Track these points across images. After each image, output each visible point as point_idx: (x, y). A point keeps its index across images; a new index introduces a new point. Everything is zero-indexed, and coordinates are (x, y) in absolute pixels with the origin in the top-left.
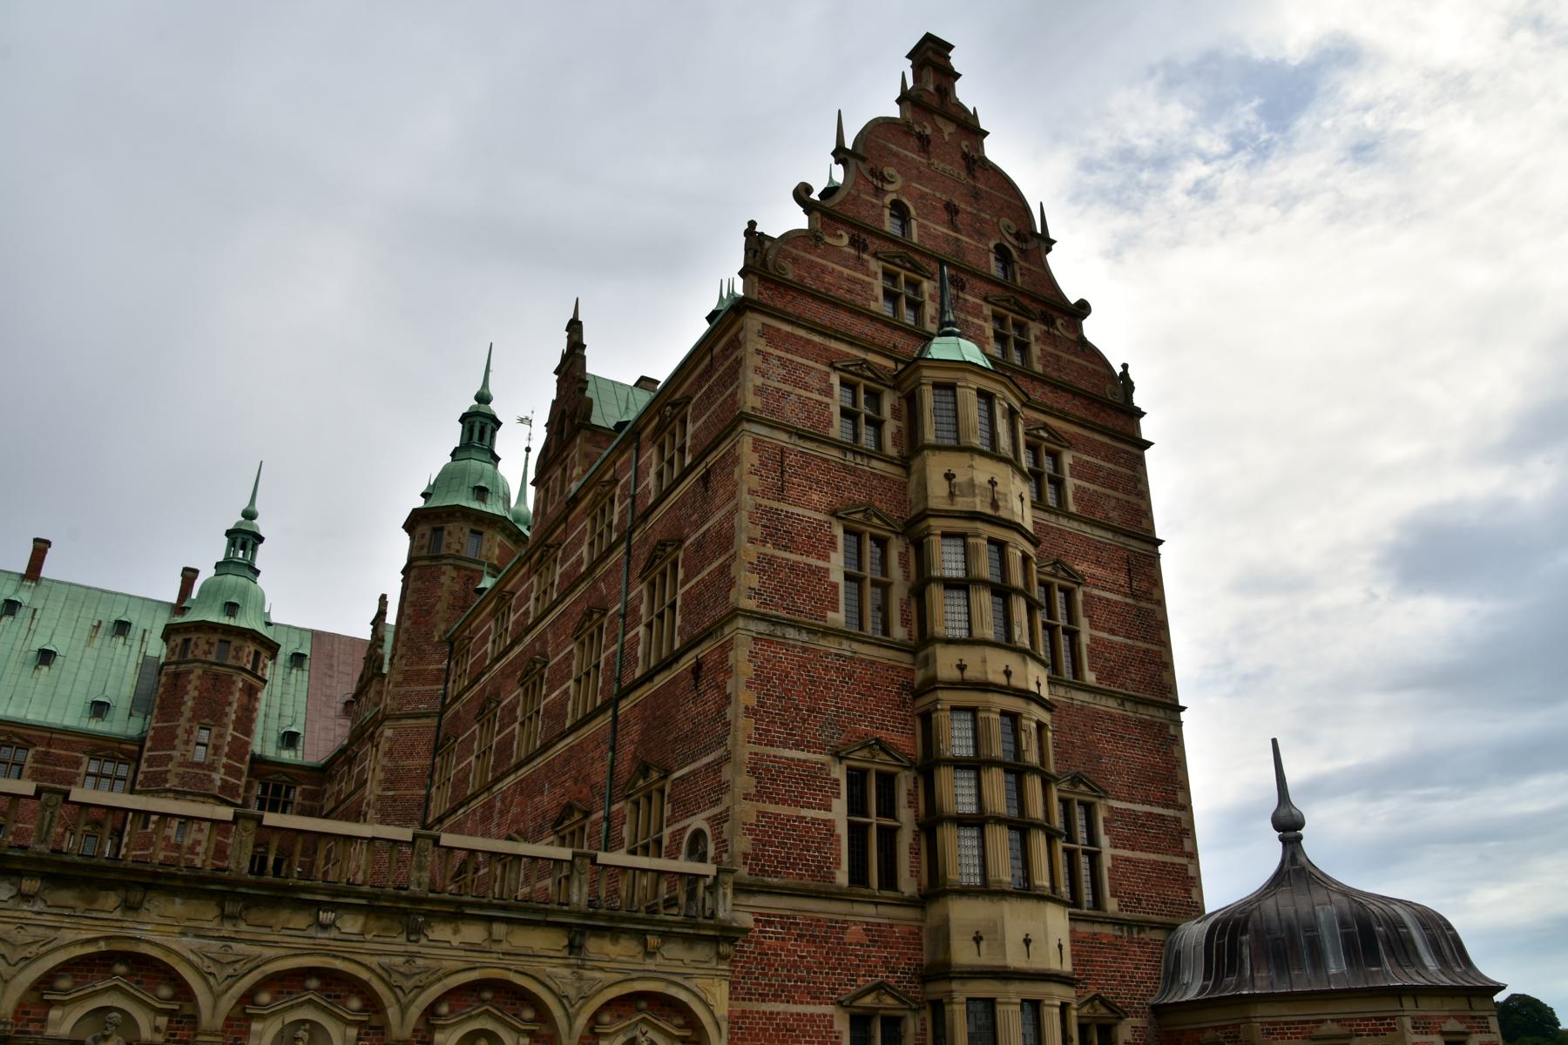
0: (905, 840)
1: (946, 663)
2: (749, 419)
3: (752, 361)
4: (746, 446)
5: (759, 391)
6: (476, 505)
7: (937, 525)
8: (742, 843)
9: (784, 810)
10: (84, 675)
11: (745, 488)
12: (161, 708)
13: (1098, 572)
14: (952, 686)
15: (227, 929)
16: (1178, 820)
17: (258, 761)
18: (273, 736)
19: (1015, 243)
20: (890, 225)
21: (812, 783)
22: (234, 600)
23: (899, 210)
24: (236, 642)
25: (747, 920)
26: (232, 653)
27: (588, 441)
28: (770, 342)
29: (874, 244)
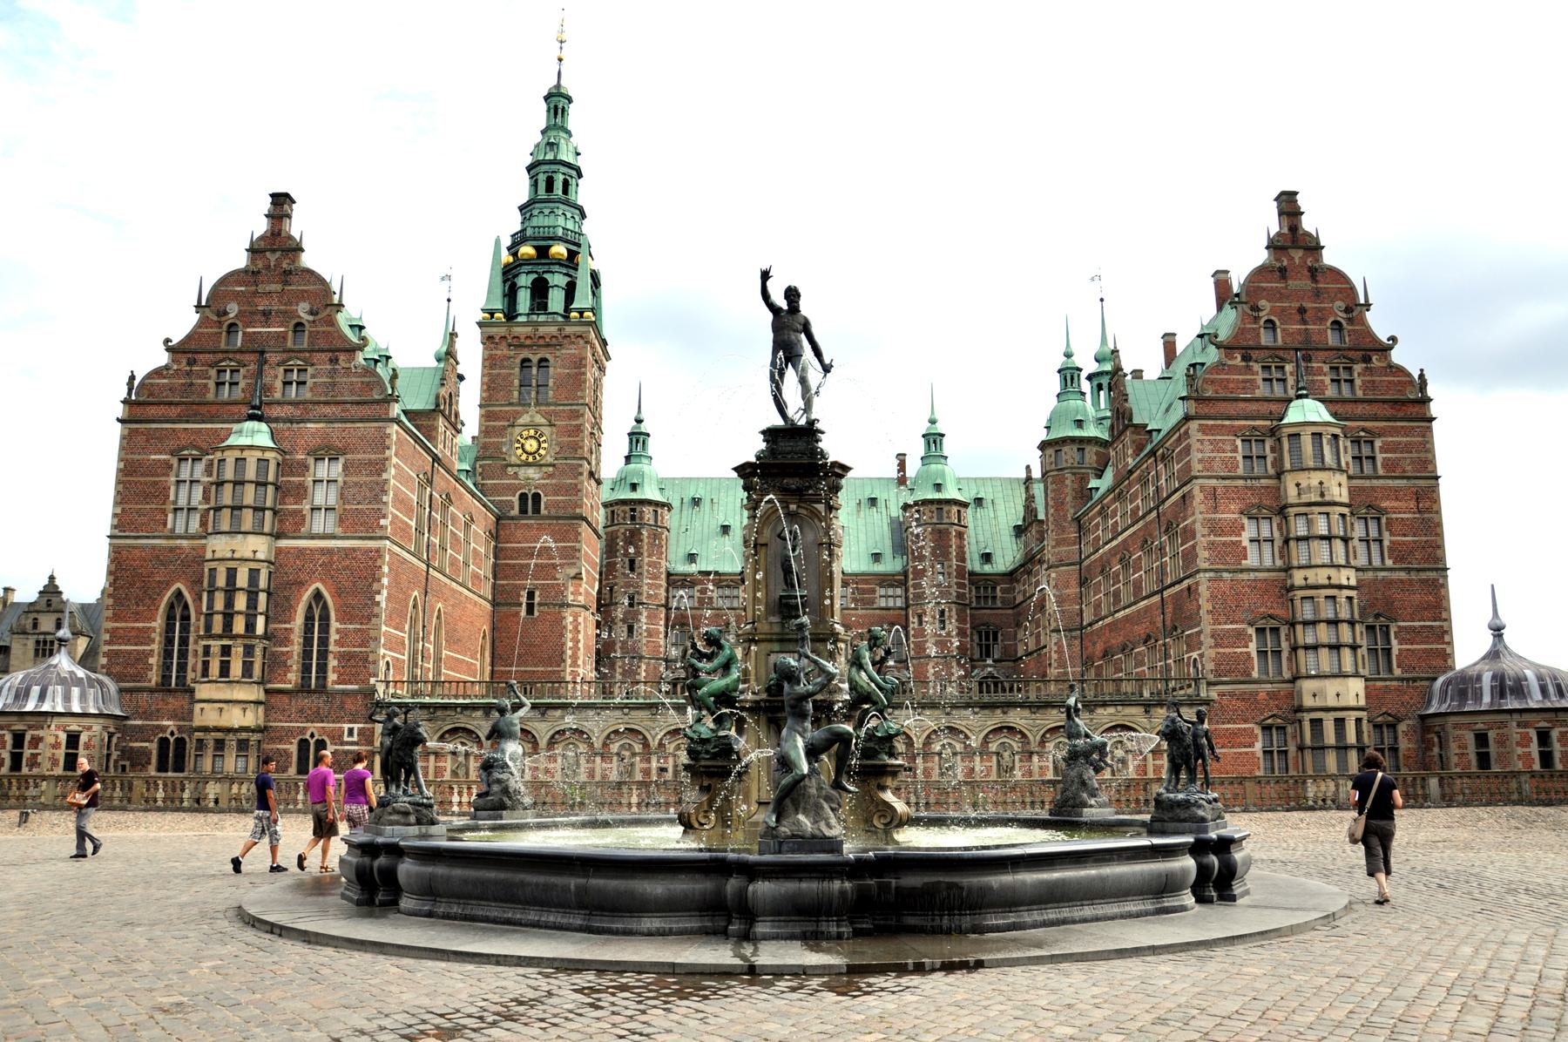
0: (1285, 655)
1: (1298, 578)
2: (1196, 478)
3: (1196, 446)
4: (1196, 491)
5: (1200, 461)
6: (1078, 433)
7: (1292, 511)
8: (1210, 666)
9: (1227, 650)
10: (862, 537)
11: (1197, 512)
13: (1396, 504)
14: (1301, 588)
15: (1033, 716)
16: (1442, 627)
17: (972, 574)
18: (976, 557)
19: (1344, 315)
20: (1265, 339)
21: (1241, 637)
22: (939, 481)
23: (1270, 325)
24: (946, 508)
25: (1214, 695)
26: (945, 515)
27: (1133, 433)
28: (1204, 433)
29: (1255, 354)
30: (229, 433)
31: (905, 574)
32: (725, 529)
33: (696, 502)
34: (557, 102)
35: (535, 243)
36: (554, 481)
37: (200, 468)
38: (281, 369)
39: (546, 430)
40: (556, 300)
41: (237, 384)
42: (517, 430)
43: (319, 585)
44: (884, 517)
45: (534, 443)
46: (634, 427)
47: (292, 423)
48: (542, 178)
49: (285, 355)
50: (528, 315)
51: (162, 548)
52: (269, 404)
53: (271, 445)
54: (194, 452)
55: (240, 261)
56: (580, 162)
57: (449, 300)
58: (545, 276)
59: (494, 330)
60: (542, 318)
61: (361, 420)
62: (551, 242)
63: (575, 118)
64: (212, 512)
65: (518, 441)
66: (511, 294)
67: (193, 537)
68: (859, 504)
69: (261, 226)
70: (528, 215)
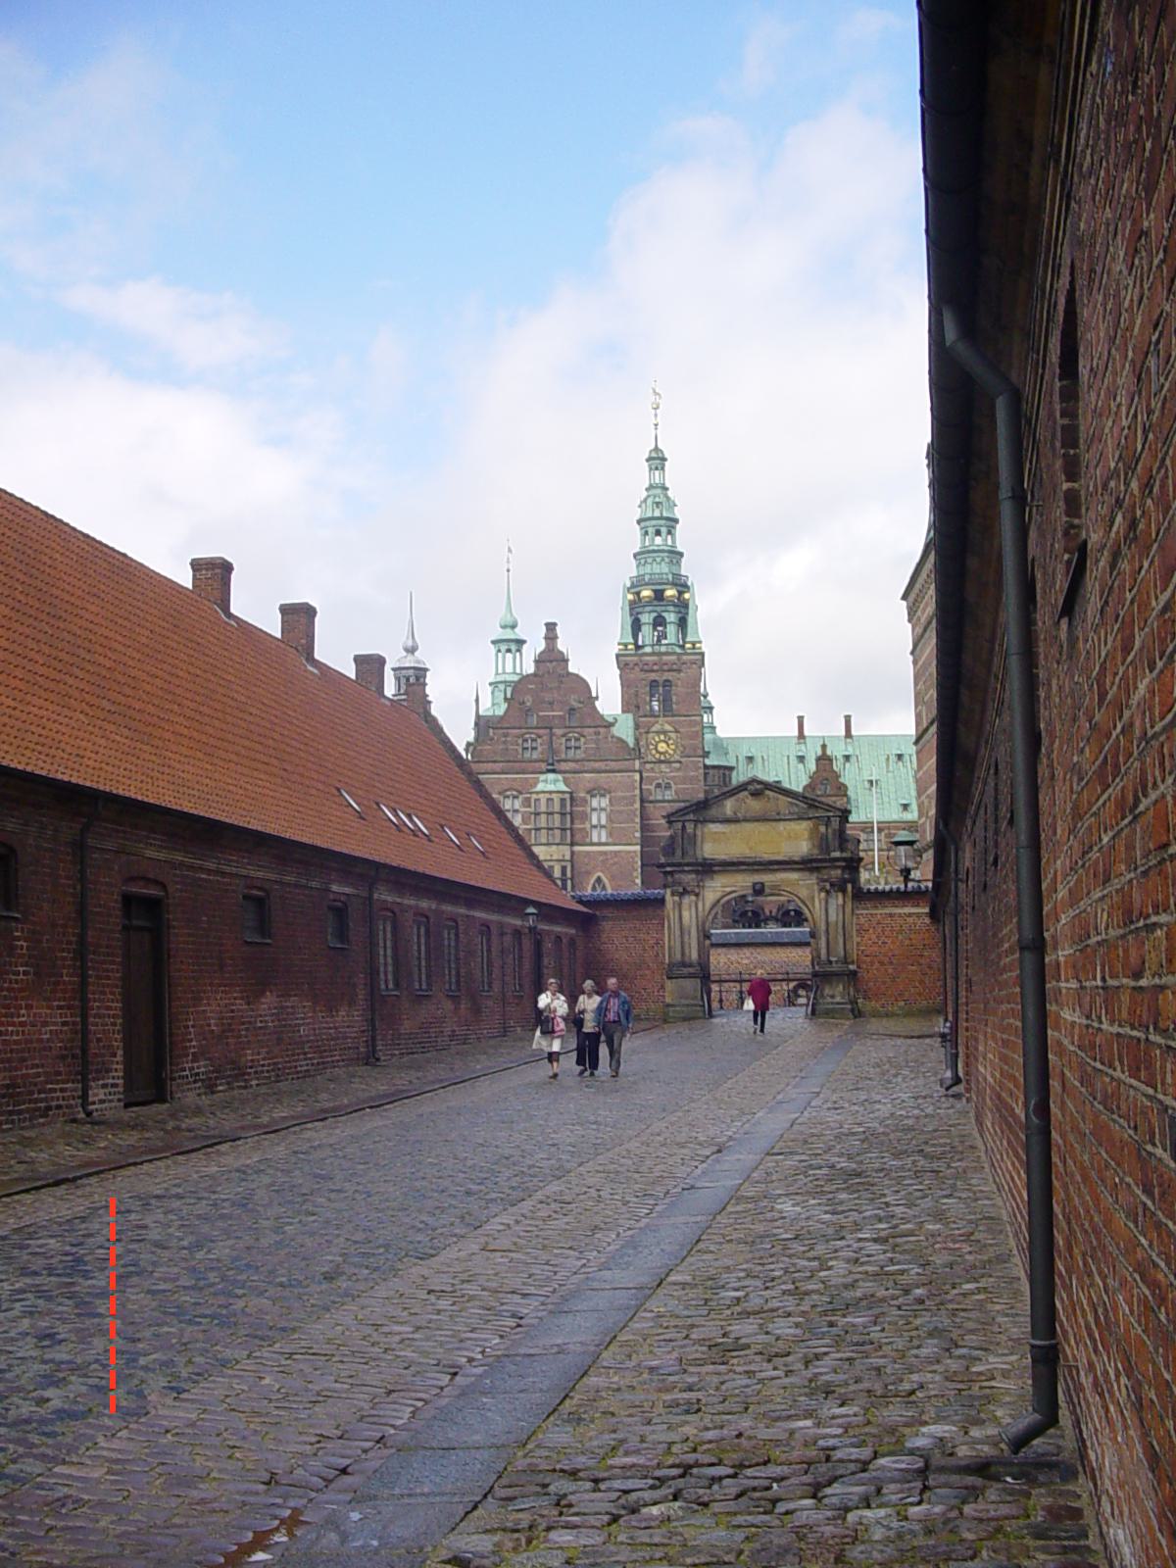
34: (657, 460)
35: (654, 587)
37: (517, 804)
38: (564, 740)
39: (673, 735)
40: (671, 630)
42: (651, 735)
43: (600, 874)
45: (664, 745)
48: (651, 530)
50: (653, 645)
52: (559, 761)
53: (565, 789)
56: (677, 514)
57: (508, 571)
58: (664, 614)
61: (618, 771)
63: (671, 476)
68: (888, 759)
70: (643, 561)
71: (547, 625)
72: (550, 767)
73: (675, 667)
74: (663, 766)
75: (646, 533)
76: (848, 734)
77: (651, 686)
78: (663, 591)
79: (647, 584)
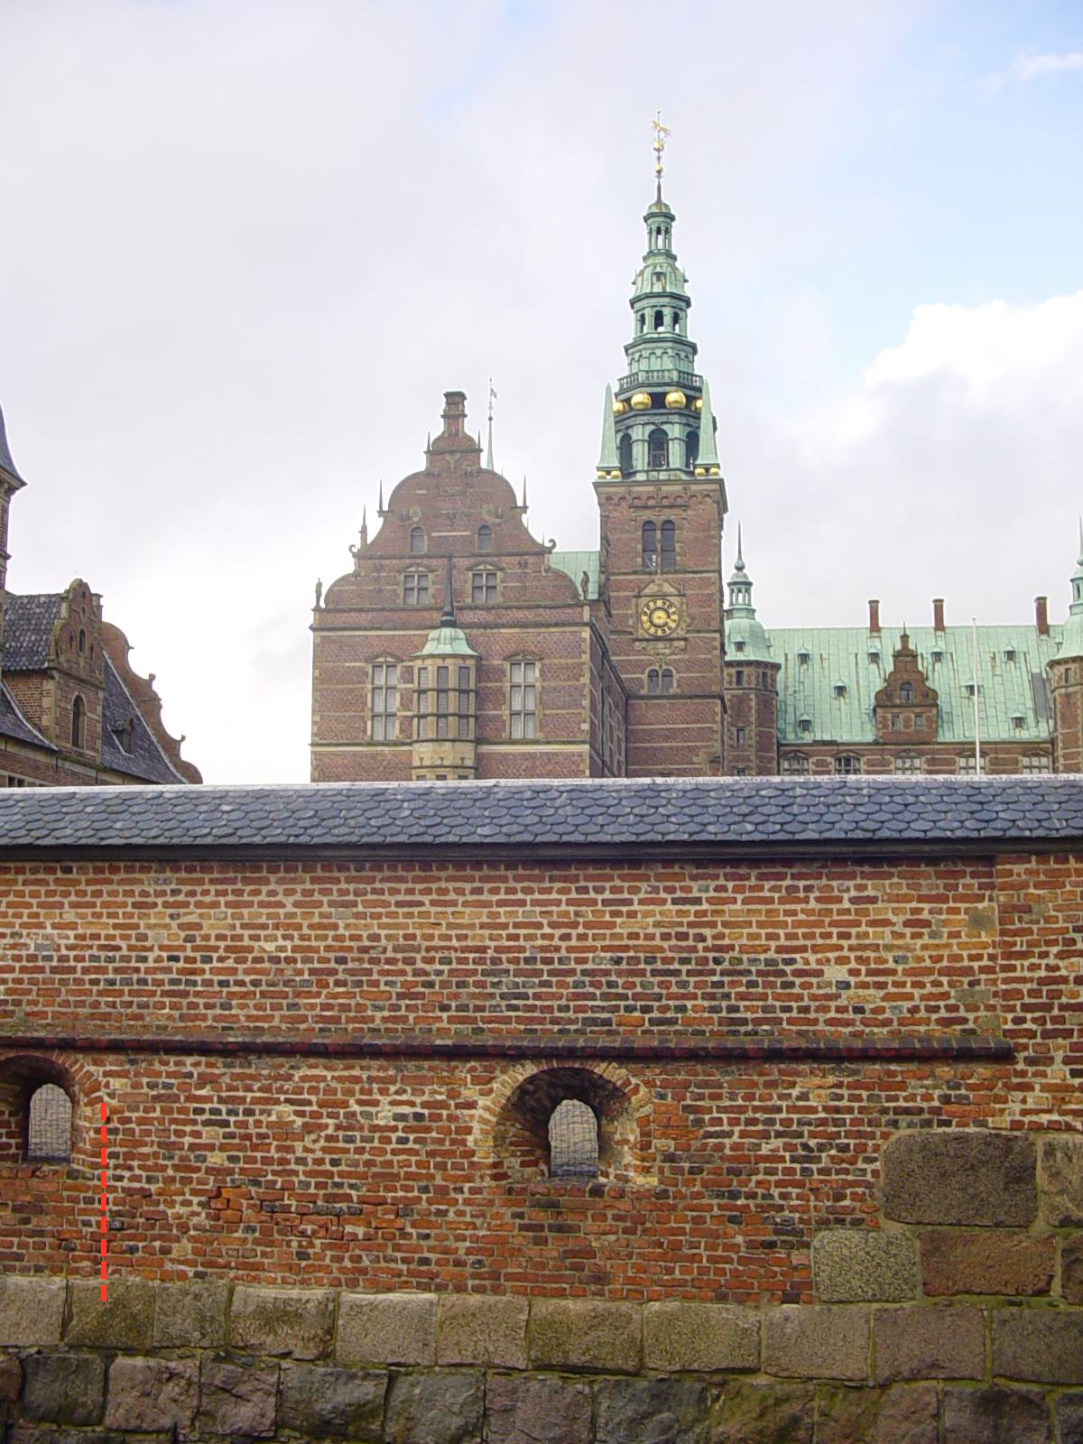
12: (1062, 719)
30: (425, 639)
31: (1053, 742)
32: (841, 690)
33: (804, 658)
34: (661, 220)
35: (650, 390)
36: (686, 657)
38: (470, 574)
41: (426, 589)
42: (643, 601)
44: (1025, 674)
45: (662, 614)
46: (737, 576)
47: (485, 628)
48: (649, 314)
49: (473, 560)
50: (647, 472)
51: (363, 755)
52: (461, 609)
53: (470, 652)
54: (389, 659)
55: (420, 464)
56: (688, 290)
57: (490, 419)
58: (665, 427)
59: (613, 489)
60: (663, 476)
61: (556, 625)
62: (667, 389)
64: (416, 720)
65: (645, 613)
66: (625, 446)
67: (395, 744)
68: (994, 658)
69: (438, 428)
70: (636, 356)
71: (448, 395)
72: (445, 618)
73: (679, 501)
74: (660, 645)
75: (642, 320)
76: (939, 625)
77: (644, 530)
78: (665, 394)
79: (641, 386)
